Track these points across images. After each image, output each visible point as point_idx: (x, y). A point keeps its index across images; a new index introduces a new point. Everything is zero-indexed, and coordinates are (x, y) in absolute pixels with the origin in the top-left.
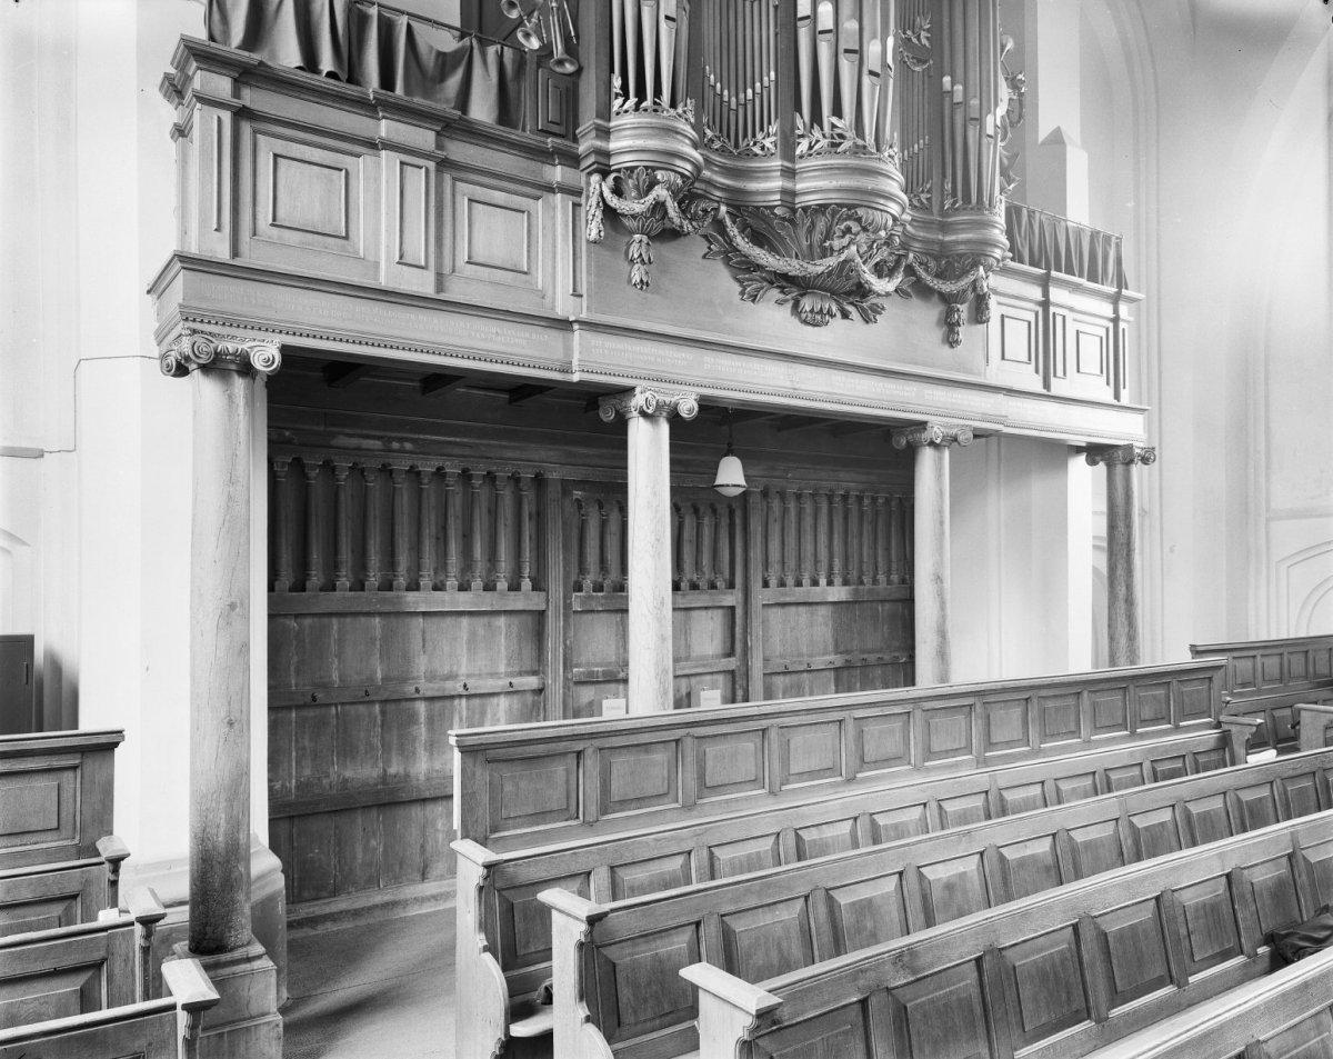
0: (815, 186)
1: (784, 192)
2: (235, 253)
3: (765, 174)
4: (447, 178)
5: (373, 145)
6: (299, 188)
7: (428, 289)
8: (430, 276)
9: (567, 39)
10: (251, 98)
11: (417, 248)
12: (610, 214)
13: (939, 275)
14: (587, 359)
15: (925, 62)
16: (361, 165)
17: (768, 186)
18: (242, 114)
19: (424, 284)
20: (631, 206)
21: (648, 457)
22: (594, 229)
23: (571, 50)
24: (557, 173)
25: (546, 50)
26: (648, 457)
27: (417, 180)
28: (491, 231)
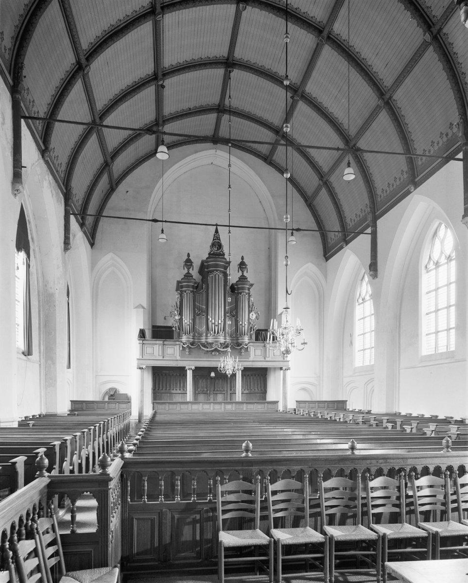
0: (210, 340)
1: (206, 341)
3: (202, 339)
6: (149, 350)
8: (162, 357)
13: (237, 346)
14: (180, 364)
16: (155, 346)
17: (203, 340)
19: (161, 358)
20: (185, 346)
21: (189, 374)
22: (181, 349)
23: (179, 329)
24: (177, 343)
25: (176, 329)
26: (189, 374)
27: (160, 347)
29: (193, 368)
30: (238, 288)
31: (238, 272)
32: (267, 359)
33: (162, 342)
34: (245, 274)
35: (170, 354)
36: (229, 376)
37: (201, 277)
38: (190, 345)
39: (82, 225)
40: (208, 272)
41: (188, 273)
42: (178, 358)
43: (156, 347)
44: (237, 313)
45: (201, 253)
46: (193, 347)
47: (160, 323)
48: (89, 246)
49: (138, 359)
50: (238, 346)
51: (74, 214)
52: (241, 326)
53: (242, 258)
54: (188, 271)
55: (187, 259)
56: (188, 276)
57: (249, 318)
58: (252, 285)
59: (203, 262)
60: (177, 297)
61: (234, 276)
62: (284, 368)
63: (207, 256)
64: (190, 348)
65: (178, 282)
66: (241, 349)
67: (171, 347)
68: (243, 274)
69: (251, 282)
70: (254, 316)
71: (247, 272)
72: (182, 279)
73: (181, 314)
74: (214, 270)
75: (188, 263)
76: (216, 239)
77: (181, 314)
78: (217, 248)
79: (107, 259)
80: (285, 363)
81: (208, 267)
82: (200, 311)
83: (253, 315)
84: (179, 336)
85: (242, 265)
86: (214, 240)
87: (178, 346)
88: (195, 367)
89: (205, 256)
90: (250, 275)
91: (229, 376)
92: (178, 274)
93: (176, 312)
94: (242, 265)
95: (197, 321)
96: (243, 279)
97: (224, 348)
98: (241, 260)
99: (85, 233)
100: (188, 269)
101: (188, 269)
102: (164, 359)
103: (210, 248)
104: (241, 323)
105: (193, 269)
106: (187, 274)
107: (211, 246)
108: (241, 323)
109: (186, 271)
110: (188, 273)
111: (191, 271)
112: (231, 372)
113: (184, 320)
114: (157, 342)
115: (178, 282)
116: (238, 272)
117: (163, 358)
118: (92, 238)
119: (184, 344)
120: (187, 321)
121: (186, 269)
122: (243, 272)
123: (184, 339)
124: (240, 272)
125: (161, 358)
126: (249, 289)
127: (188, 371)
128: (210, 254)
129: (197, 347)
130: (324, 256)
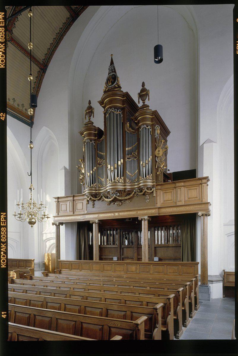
2: (58, 214)
7: (72, 214)
15: (136, 158)
27: (71, 203)
32: (179, 204)
50: (141, 192)
66: (144, 194)
71: (149, 100)
76: (111, 73)
83: (159, 151)
86: (109, 74)
97: (126, 196)
102: (74, 214)
117: (73, 213)
125: (72, 214)
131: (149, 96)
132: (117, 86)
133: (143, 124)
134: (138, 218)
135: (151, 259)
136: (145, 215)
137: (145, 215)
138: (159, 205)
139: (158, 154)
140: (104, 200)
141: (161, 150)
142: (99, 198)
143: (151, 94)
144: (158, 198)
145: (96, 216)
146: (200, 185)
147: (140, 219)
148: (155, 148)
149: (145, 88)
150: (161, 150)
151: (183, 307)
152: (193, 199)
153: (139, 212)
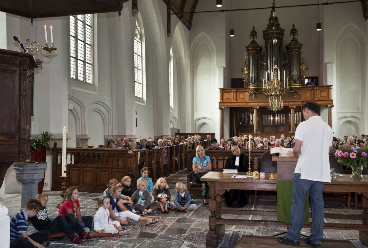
4: (237, 93)
5: (232, 92)
6: (227, 96)
7: (236, 102)
9: (247, 79)
10: (223, 91)
11: (235, 98)
12: (250, 93)
13: (291, 91)
16: (231, 93)
18: (223, 92)
19: (235, 101)
22: (249, 94)
24: (247, 90)
25: (245, 80)
28: (241, 96)
29: (258, 107)
30: (291, 48)
31: (291, 36)
32: (315, 99)
33: (235, 90)
34: (296, 37)
35: (244, 98)
36: (275, 112)
37: (263, 41)
38: (255, 92)
39: (180, 18)
40: (268, 38)
41: (254, 40)
42: (248, 101)
43: (232, 94)
44: (290, 67)
45: (262, 24)
46: (258, 93)
47: (237, 76)
48: (187, 30)
49: (219, 102)
51: (175, 13)
52: (293, 76)
53: (294, 26)
54: (254, 39)
55: (253, 31)
56: (254, 43)
57: (300, 69)
58: (302, 45)
59: (264, 32)
60: (246, 58)
61: (287, 39)
62: (329, 106)
63: (267, 27)
64: (255, 94)
65: (247, 47)
66: (294, 92)
67: (242, 93)
68: (294, 37)
69: (301, 43)
70: (304, 68)
72: (249, 45)
73: (248, 70)
74: (272, 37)
75: (254, 34)
77: (248, 70)
78: (274, 21)
79: (201, 35)
80: (330, 102)
81: (268, 35)
82: (260, 68)
83: (303, 67)
84: (248, 85)
85: (294, 31)
87: (247, 93)
88: (260, 107)
89: (265, 27)
90: (300, 38)
91: (275, 112)
92: (248, 41)
93: (245, 69)
94: (294, 31)
95: (261, 74)
96: (294, 40)
98: (293, 27)
99: (183, 22)
100: (254, 38)
101: (254, 38)
102: (237, 102)
103: (268, 21)
104: (293, 73)
105: (257, 38)
106: (253, 41)
107: (269, 20)
108: (293, 73)
109: (252, 39)
110: (254, 40)
111: (255, 39)
112: (277, 110)
113: (251, 74)
114: (233, 90)
115: (247, 47)
116: (291, 36)
117: (237, 101)
118: (188, 24)
119: (251, 91)
120: (252, 75)
121: (252, 38)
122: (294, 36)
123: (252, 87)
124: (292, 36)
126: (300, 48)
127: (255, 110)
128: (268, 26)
129: (260, 93)
130: (364, 16)
131: (257, 35)
132: (277, 24)
133: (295, 50)
134: (289, 106)
135: (257, 132)
136: (294, 105)
137: (294, 105)
138: (302, 100)
139: (302, 68)
140: (263, 93)
141: (304, 66)
142: (259, 92)
143: (298, 32)
144: (302, 95)
145: (257, 104)
146: (328, 90)
147: (290, 107)
148: (300, 65)
149: (295, 28)
150: (304, 66)
151: (170, 161)
152: (324, 97)
153: (290, 103)
